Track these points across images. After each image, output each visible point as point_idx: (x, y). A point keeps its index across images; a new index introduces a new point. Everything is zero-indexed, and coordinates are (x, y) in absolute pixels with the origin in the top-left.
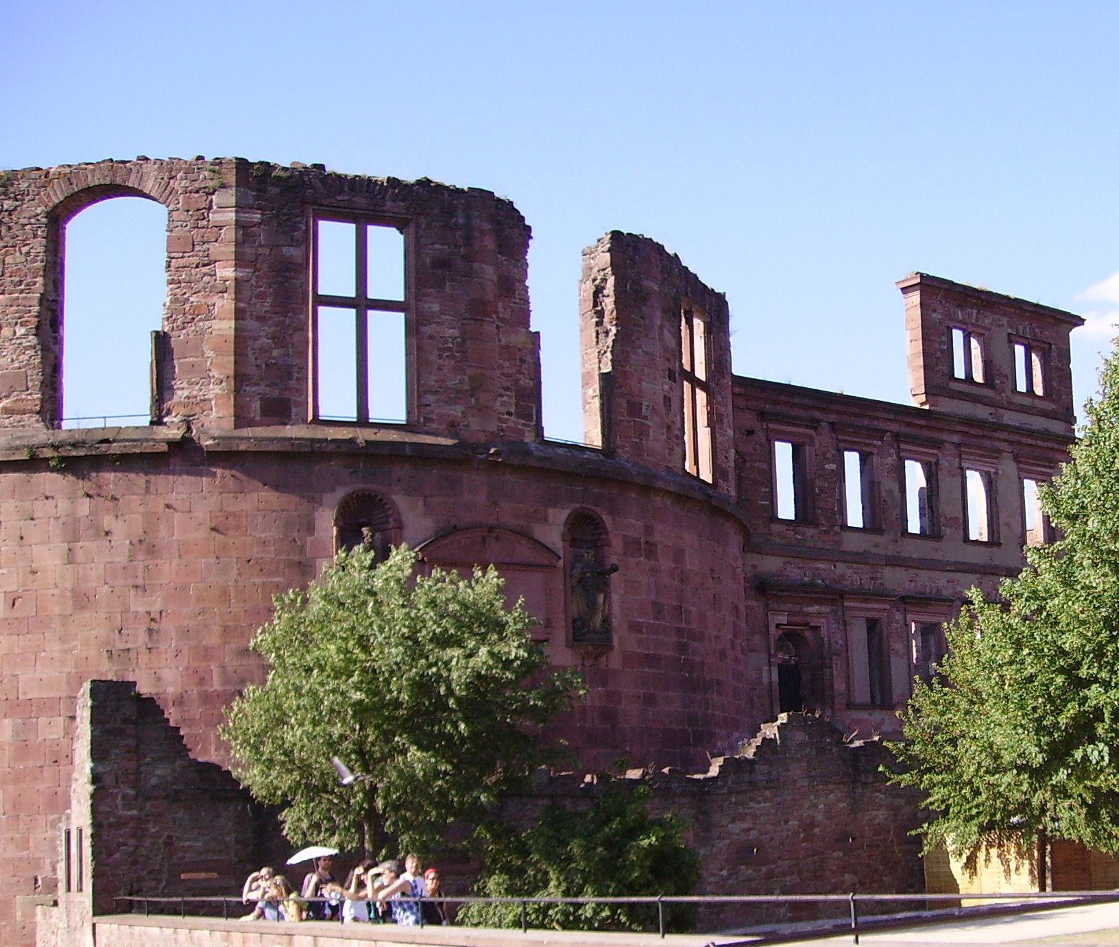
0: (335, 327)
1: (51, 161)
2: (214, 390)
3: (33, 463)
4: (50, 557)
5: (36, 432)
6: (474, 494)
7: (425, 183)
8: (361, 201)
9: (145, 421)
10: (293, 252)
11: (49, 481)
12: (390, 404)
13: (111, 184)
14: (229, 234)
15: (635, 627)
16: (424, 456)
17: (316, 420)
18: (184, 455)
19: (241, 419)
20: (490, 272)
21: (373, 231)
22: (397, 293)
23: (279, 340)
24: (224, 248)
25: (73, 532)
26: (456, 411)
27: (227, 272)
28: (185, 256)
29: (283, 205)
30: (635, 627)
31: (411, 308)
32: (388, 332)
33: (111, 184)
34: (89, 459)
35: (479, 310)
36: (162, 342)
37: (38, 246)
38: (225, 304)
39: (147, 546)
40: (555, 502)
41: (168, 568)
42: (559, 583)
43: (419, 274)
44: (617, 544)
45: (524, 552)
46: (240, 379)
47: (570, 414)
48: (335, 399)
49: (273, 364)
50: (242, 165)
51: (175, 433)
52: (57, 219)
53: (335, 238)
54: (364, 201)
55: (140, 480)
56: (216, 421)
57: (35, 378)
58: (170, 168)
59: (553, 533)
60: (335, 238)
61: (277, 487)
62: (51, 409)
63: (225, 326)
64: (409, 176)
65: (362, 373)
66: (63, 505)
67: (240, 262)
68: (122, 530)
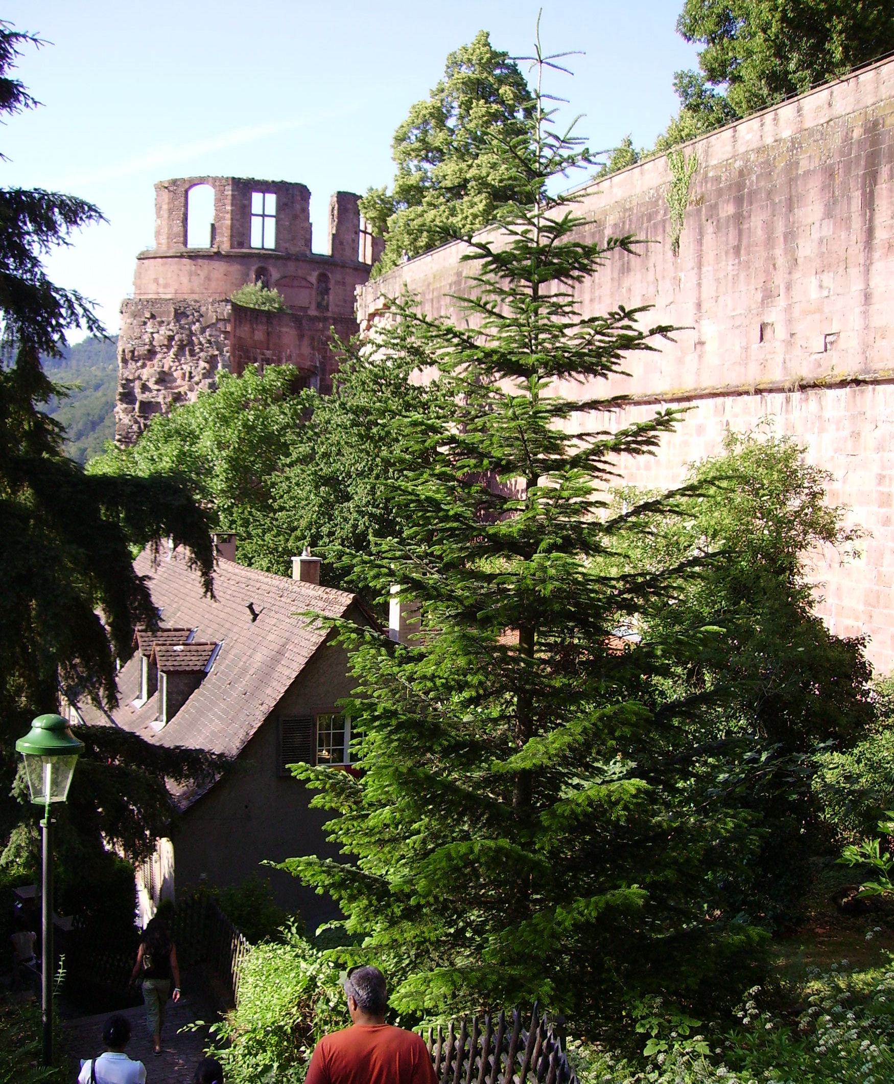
0: (256, 222)
1: (186, 176)
2: (225, 239)
3: (181, 256)
4: (185, 280)
5: (182, 248)
6: (291, 268)
7: (282, 182)
8: (264, 187)
9: (208, 246)
10: (246, 202)
11: (186, 261)
12: (270, 243)
13: (201, 181)
14: (230, 197)
15: (337, 306)
16: (277, 258)
17: (251, 248)
18: (218, 256)
19: (232, 247)
20: (298, 207)
21: (267, 195)
22: (274, 213)
23: (242, 226)
24: (228, 201)
25: (191, 274)
26: (287, 245)
27: (229, 208)
28: (219, 201)
29: (243, 189)
30: (337, 306)
31: (277, 217)
32: (271, 224)
33: (201, 181)
34: (195, 256)
35: (295, 217)
36: (213, 225)
37: (182, 199)
38: (228, 216)
39: (208, 278)
40: (314, 270)
41: (213, 285)
42: (314, 292)
43: (280, 207)
44: (332, 282)
45: (304, 283)
46: (232, 236)
47: (322, 245)
48: (256, 242)
49: (241, 233)
50: (233, 178)
51: (215, 250)
52: (186, 192)
53: (257, 197)
54: (265, 187)
55: (206, 262)
56: (225, 247)
57: (182, 234)
58: (215, 179)
59: (313, 278)
60: (257, 197)
61: (241, 264)
62: (185, 243)
63: (228, 222)
64: (278, 179)
65: (264, 235)
66: (188, 267)
67: (232, 205)
68: (203, 274)
